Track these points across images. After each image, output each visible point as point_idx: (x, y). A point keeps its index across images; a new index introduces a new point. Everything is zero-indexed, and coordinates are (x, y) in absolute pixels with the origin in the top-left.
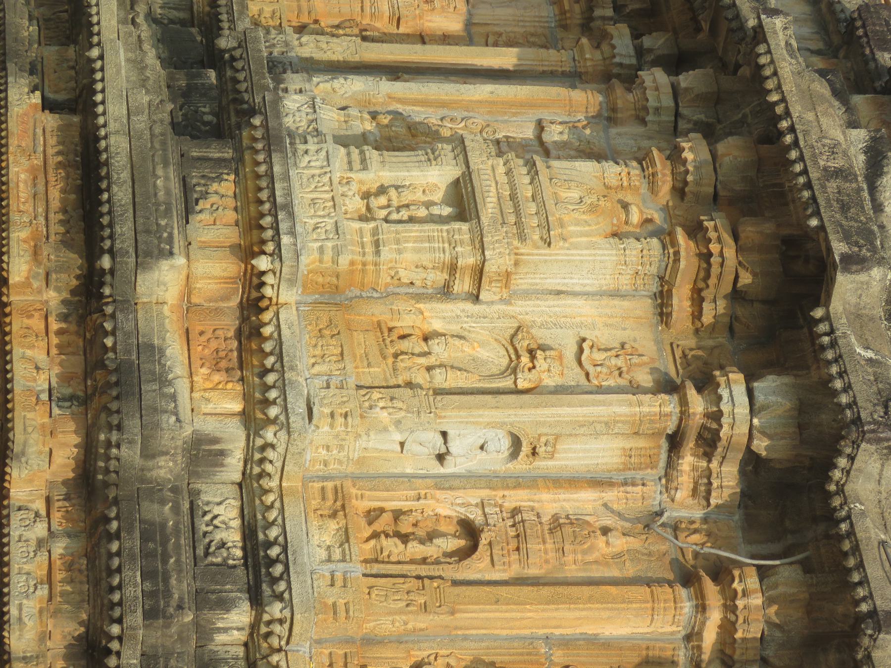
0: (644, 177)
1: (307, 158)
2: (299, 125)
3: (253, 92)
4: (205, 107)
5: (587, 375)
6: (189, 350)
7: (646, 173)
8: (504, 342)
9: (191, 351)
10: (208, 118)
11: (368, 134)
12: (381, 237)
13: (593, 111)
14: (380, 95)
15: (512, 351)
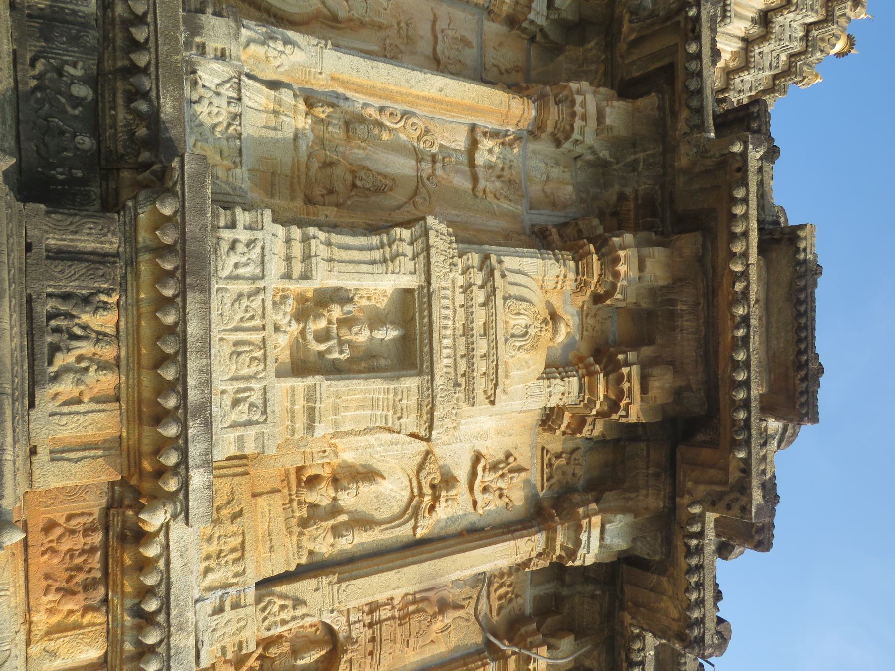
0: (576, 281)
1: (233, 259)
2: (216, 121)
3: (157, 79)
4: (74, 65)
5: (475, 503)
6: (26, 560)
7: (579, 278)
8: (410, 472)
9: (31, 568)
10: (81, 91)
11: (300, 135)
12: (317, 406)
13: (524, 125)
14: (323, 75)
15: (415, 484)
